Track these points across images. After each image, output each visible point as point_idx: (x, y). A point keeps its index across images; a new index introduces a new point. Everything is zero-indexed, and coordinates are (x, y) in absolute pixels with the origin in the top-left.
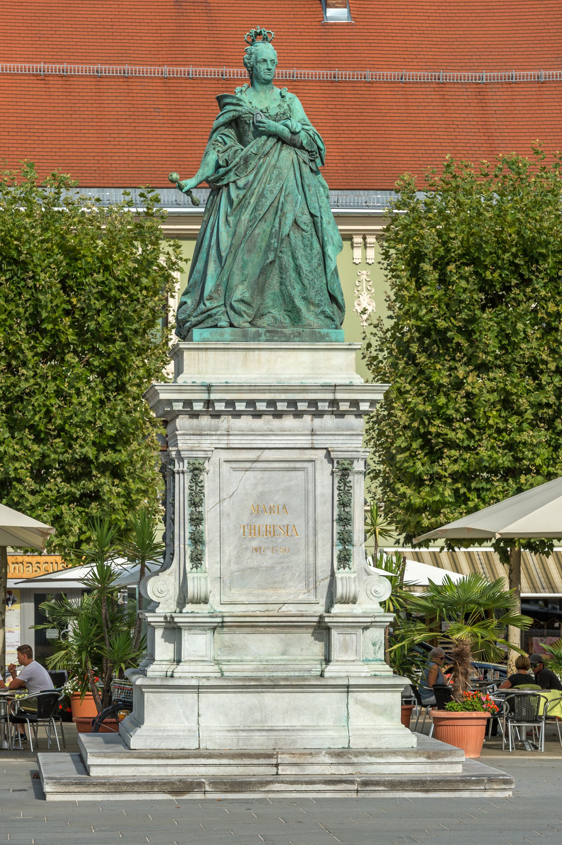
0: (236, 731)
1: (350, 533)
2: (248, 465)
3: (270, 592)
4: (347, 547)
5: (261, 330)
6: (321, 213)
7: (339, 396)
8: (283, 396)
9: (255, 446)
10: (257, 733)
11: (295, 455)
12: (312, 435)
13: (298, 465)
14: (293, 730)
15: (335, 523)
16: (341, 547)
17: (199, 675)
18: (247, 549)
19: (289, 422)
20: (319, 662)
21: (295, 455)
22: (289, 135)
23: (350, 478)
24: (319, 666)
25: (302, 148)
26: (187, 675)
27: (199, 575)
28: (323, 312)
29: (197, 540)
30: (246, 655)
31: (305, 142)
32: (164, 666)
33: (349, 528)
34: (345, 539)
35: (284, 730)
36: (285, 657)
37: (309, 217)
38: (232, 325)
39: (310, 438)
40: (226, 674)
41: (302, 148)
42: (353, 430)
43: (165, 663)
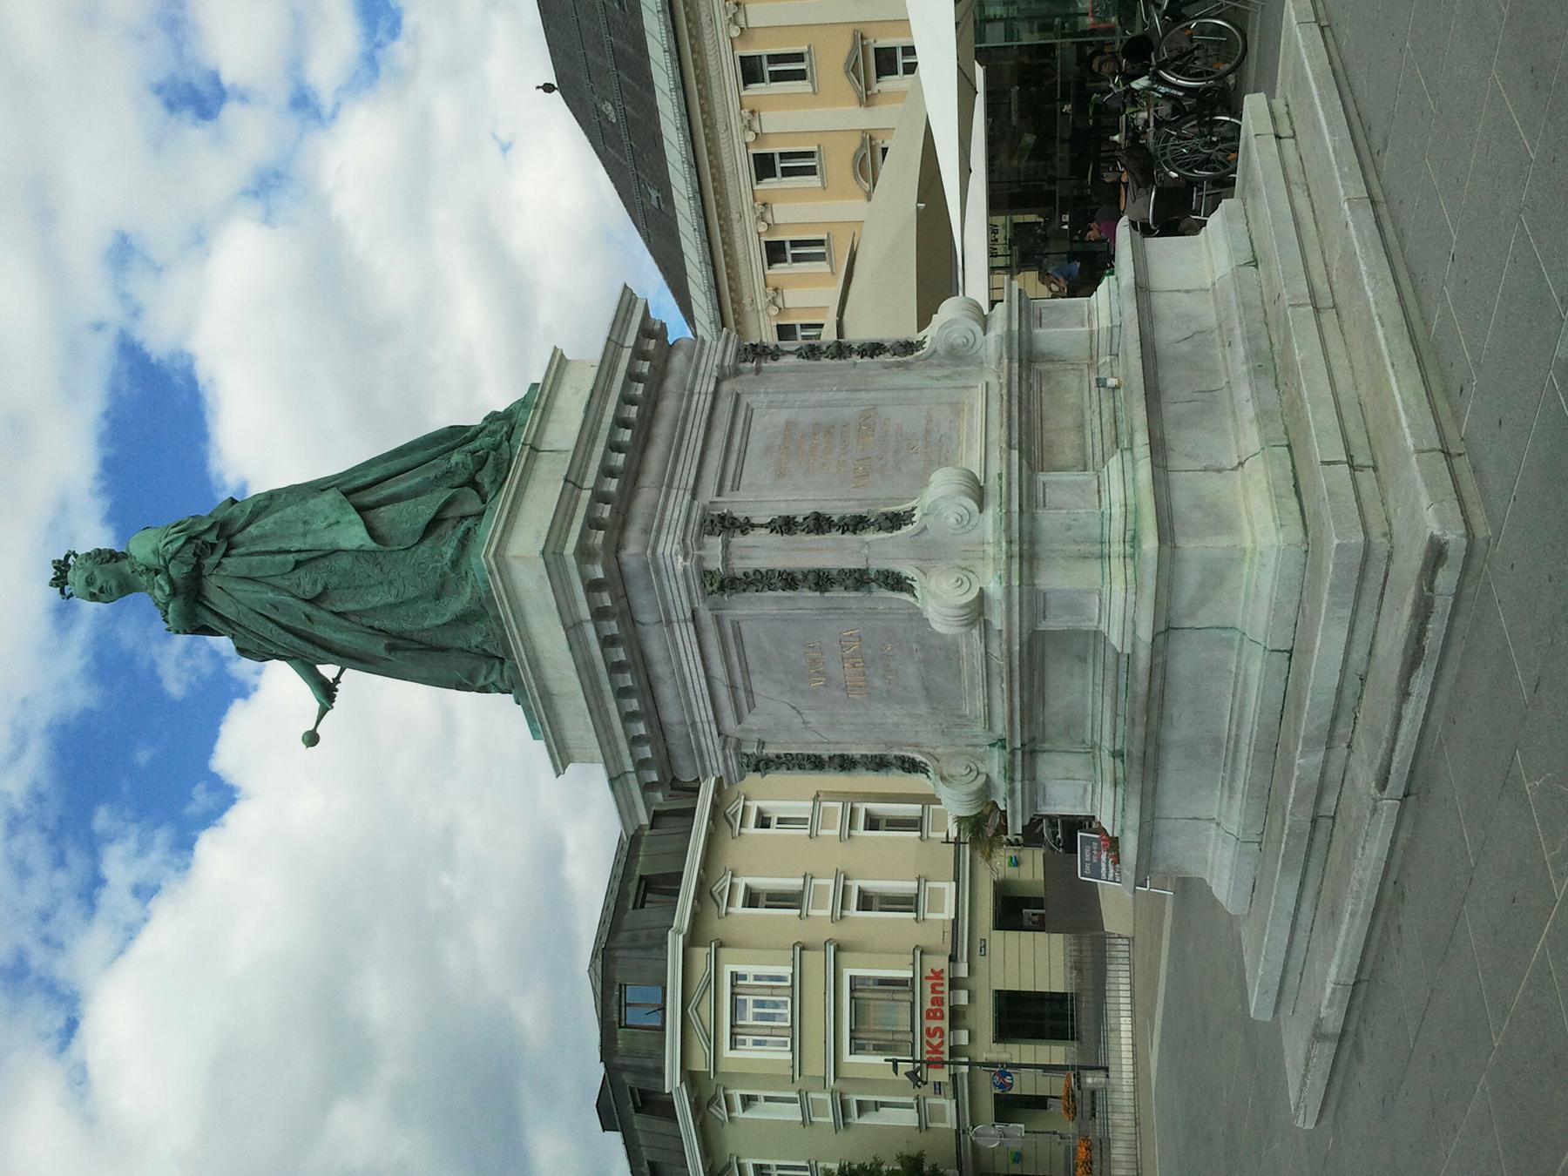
2: (742, 694)
3: (965, 668)
6: (289, 552)
7: (584, 611)
8: (607, 687)
9: (706, 692)
11: (712, 639)
12: (669, 623)
13: (730, 632)
18: (888, 692)
19: (655, 649)
21: (712, 639)
23: (739, 574)
25: (198, 568)
28: (455, 563)
30: (1084, 706)
34: (859, 580)
36: (1090, 659)
37: (301, 572)
39: (676, 626)
41: (198, 568)
42: (647, 568)
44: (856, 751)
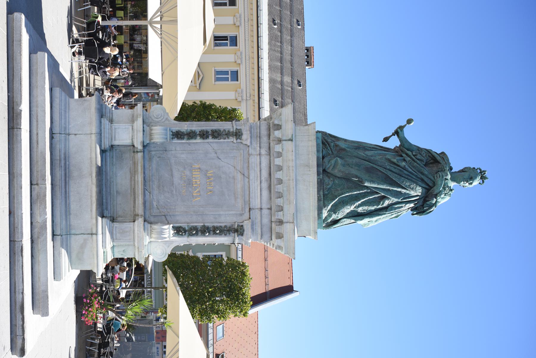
0: (65, 159)
1: (196, 234)
4: (187, 233)
5: (321, 176)
10: (63, 173)
14: (66, 198)
15: (202, 224)
16: (187, 228)
17: (103, 135)
19: (265, 193)
20: (112, 215)
22: (435, 193)
24: (109, 215)
26: (103, 127)
27: (169, 136)
29: (191, 135)
31: (428, 203)
32: (108, 115)
33: (200, 234)
35: (66, 192)
36: (115, 194)
38: (323, 158)
40: (104, 154)
43: (111, 116)
44: (199, 140)
